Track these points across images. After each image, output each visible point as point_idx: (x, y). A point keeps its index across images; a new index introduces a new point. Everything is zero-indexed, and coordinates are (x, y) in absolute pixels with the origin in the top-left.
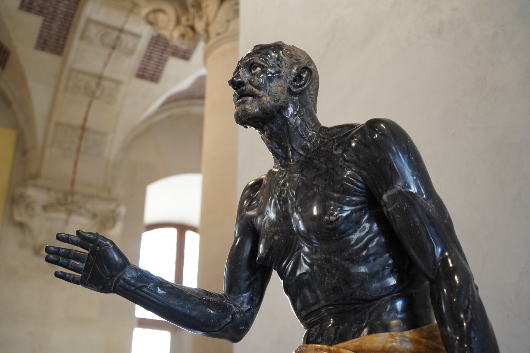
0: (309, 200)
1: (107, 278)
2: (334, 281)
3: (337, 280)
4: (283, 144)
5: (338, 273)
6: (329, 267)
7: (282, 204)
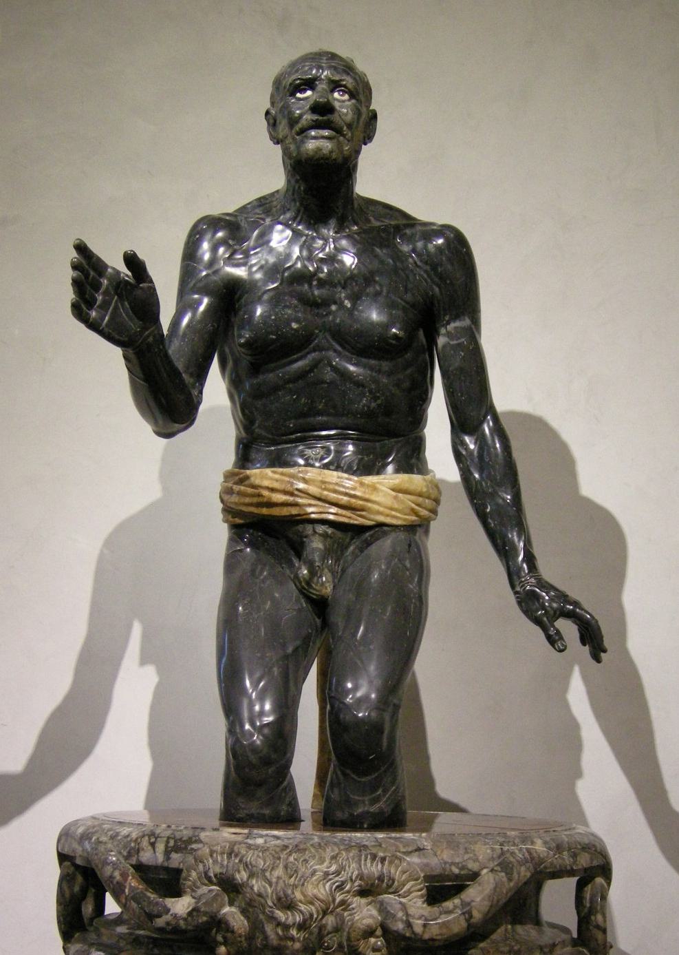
2: (373, 405)
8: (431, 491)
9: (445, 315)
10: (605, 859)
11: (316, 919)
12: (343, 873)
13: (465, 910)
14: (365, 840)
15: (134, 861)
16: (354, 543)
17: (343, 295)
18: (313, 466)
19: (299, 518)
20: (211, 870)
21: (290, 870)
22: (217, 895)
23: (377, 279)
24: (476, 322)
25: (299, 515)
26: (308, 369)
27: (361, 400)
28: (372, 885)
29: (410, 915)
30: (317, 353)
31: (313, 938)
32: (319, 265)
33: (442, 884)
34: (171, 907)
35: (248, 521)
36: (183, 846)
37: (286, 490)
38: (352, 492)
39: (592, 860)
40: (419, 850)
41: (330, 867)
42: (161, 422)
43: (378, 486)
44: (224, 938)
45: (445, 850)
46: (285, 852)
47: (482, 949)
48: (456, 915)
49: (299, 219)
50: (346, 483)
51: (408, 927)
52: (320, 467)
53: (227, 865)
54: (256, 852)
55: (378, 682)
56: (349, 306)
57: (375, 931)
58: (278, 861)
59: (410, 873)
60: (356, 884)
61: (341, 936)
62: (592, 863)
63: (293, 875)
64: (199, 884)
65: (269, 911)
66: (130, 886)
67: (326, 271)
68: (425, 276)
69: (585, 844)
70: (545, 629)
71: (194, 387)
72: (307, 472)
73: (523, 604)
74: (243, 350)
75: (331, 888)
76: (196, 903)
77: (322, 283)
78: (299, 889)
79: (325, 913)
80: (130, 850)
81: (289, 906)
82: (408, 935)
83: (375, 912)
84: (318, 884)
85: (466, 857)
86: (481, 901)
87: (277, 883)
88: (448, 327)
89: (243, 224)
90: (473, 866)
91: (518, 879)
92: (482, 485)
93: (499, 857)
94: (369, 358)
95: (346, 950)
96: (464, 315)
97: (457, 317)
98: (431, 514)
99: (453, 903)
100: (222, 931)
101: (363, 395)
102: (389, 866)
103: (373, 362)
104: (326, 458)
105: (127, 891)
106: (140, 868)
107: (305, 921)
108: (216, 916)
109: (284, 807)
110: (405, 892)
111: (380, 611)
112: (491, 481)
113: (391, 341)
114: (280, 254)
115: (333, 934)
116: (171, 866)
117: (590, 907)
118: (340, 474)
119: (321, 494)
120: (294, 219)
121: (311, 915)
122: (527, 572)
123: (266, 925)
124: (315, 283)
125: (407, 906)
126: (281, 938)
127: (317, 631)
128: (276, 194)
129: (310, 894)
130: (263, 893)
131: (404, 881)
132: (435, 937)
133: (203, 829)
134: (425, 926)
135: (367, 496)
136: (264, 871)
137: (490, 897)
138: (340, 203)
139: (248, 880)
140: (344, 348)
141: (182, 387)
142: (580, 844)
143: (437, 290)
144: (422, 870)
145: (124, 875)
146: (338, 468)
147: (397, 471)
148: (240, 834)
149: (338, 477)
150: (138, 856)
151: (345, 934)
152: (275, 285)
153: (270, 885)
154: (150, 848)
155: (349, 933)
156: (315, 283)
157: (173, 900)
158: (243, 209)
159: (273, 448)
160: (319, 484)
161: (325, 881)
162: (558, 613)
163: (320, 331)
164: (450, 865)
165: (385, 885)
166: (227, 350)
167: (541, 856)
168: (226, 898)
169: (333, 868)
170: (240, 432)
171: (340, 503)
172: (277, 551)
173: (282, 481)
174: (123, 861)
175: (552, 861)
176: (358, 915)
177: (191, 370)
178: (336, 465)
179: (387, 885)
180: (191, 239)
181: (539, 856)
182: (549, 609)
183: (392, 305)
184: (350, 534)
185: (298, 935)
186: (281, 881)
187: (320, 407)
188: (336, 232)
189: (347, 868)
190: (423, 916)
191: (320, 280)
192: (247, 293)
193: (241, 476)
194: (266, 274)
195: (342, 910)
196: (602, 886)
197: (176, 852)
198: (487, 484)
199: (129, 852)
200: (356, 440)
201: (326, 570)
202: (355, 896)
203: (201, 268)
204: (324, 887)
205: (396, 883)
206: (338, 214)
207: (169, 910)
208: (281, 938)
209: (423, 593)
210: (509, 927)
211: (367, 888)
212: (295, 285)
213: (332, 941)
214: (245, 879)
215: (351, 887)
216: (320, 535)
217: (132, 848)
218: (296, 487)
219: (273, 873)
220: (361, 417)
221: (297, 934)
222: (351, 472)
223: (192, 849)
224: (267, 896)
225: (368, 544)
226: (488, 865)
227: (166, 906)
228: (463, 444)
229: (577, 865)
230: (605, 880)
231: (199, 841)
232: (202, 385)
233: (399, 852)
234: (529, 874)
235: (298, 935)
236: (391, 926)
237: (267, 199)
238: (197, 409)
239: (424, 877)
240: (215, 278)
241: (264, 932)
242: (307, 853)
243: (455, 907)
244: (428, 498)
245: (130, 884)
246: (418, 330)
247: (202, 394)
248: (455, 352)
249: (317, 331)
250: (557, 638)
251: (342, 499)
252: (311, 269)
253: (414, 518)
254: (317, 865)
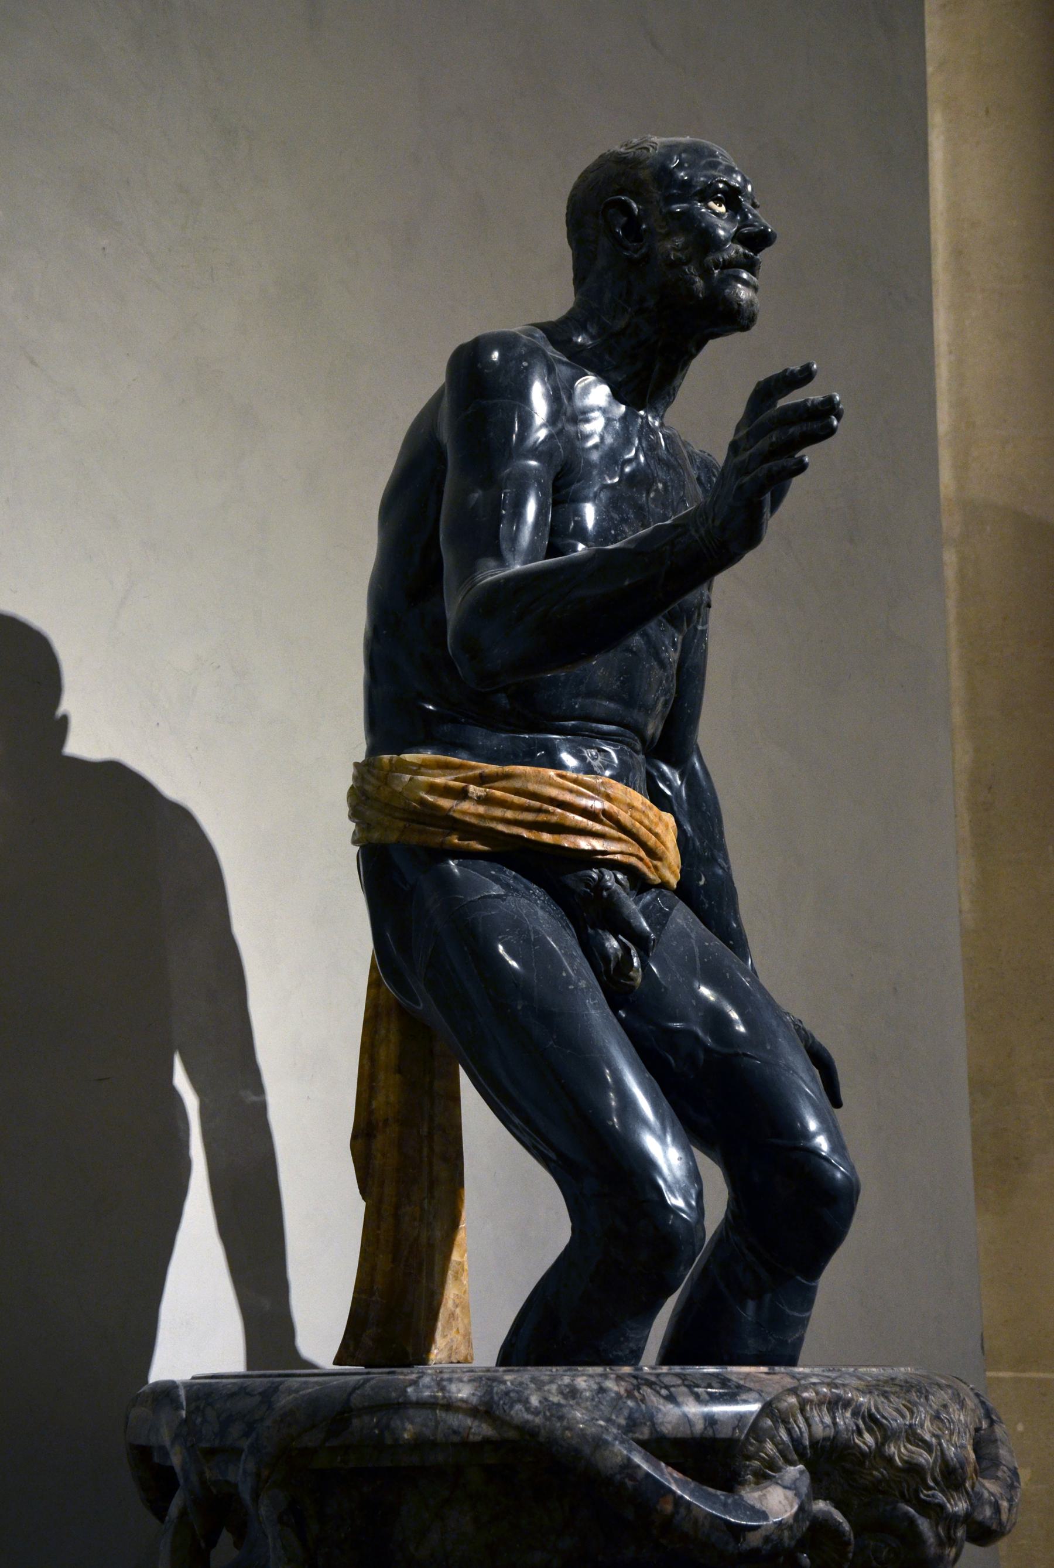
64: (781, 1462)
116: (719, 1436)
198: (702, 843)
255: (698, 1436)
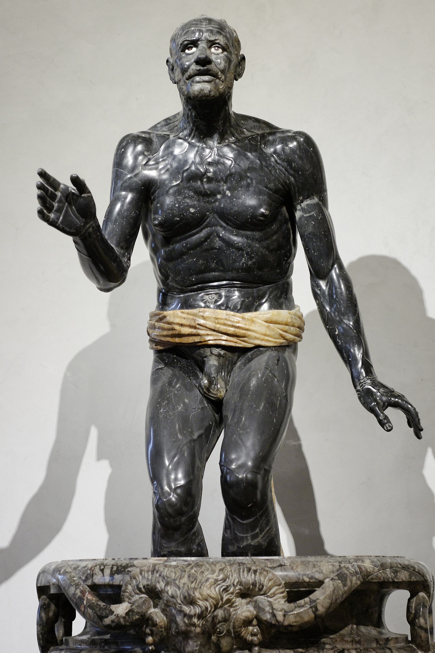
0: (242, 189)
1: (81, 223)
2: (250, 263)
3: (253, 262)
4: (215, 124)
5: (256, 257)
6: (249, 250)
7: (205, 182)
8: (294, 321)
9: (299, 197)
10: (423, 577)
11: (210, 611)
12: (228, 580)
13: (312, 605)
14: (245, 560)
15: (89, 582)
16: (241, 360)
17: (225, 187)
18: (209, 307)
19: (200, 344)
20: (141, 584)
21: (193, 578)
22: (145, 600)
23: (249, 175)
24: (323, 200)
25: (200, 342)
26: (203, 239)
27: (241, 260)
28: (249, 589)
29: (275, 609)
30: (209, 228)
31: (209, 624)
32: (207, 167)
33: (299, 589)
34: (115, 611)
35: (166, 347)
36: (122, 570)
37: (191, 325)
38: (237, 325)
39: (410, 576)
40: (281, 566)
41: (219, 576)
42: (101, 282)
43: (255, 319)
44: (151, 630)
45: (299, 566)
46: (189, 567)
47: (331, 638)
48: (306, 608)
49: (193, 135)
50: (232, 318)
51: (273, 617)
52: (214, 308)
53: (151, 579)
54: (170, 569)
55: (252, 454)
56: (229, 195)
57: (252, 620)
58: (184, 573)
59: (274, 581)
60: (238, 588)
61: (229, 625)
62: (411, 579)
63: (193, 581)
65: (178, 607)
66: (87, 599)
67: (212, 170)
68: (283, 169)
69: (405, 565)
70: (377, 416)
71: (124, 255)
72: (205, 312)
73: (362, 399)
74: (157, 228)
75: (220, 590)
76: (131, 606)
77: (210, 180)
78: (198, 590)
79: (216, 607)
80: (87, 575)
81: (191, 602)
82: (273, 622)
83: (252, 609)
84: (210, 587)
85: (314, 570)
86: (324, 599)
87: (183, 587)
88: (302, 204)
89: (155, 140)
90: (318, 576)
91: (351, 585)
92: (331, 315)
93: (338, 571)
94: (245, 230)
95: (233, 635)
96: (313, 195)
97: (308, 197)
98: (295, 337)
99: (304, 601)
100: (149, 626)
101: (243, 256)
102: (259, 576)
103: (248, 233)
104: (219, 301)
105: (85, 602)
106: (94, 588)
107: (202, 612)
108: (145, 615)
109: (195, 547)
110: (271, 594)
111: (254, 406)
112: (338, 313)
113: (260, 218)
114: (180, 160)
115: (223, 623)
116: (114, 584)
117: (415, 613)
118: (228, 312)
119: (214, 327)
120: (190, 135)
121: (207, 608)
122: (364, 375)
123: (177, 617)
124: (205, 180)
125: (273, 603)
126: (187, 625)
127: (216, 422)
128: (177, 116)
129: (205, 593)
130: (175, 595)
131: (270, 586)
132: (292, 624)
133: (136, 559)
134: (284, 616)
135: (247, 327)
136: (175, 580)
137: (330, 597)
138: (220, 123)
139: (165, 587)
140: (227, 224)
141: (115, 258)
142: (401, 565)
143: (292, 179)
144: (283, 579)
145: (83, 592)
146: (227, 308)
147: (271, 308)
148: (161, 560)
149: (227, 315)
150: (92, 579)
151: (232, 624)
152: (178, 182)
153: (179, 588)
154: (100, 573)
155: (234, 623)
156: (205, 180)
157: (116, 605)
158: (155, 127)
159: (182, 296)
160: (214, 320)
161: (215, 585)
162: (386, 403)
163: (210, 213)
164: (302, 576)
165: (257, 589)
166: (147, 226)
167: (369, 570)
168: (152, 603)
169: (221, 576)
170: (159, 284)
171: (228, 332)
172: (187, 367)
173: (188, 319)
174: (83, 583)
175: (378, 574)
176: (240, 610)
177: (122, 244)
178: (225, 306)
179: (259, 588)
180: (119, 152)
181: (366, 570)
182: (380, 401)
183: (259, 193)
184: (237, 354)
185: (199, 623)
186: (186, 586)
187: (213, 266)
188: (219, 143)
189: (231, 577)
190: (284, 609)
191: (208, 178)
192: (158, 189)
193: (161, 316)
194: (171, 174)
195: (229, 606)
196: (424, 598)
197: (118, 574)
199: (86, 577)
200: (239, 288)
201: (220, 380)
202: (237, 597)
203: (126, 173)
204: (215, 590)
205: (265, 587)
206: (219, 130)
207: (113, 612)
208: (187, 625)
209: (289, 394)
210: (355, 626)
211: (245, 591)
212: (191, 182)
213: (222, 627)
214: (163, 587)
215: (234, 590)
216: (215, 355)
217: (88, 574)
218: (197, 322)
219: (181, 581)
220: (242, 272)
221: (198, 622)
222: (236, 311)
223: (128, 571)
224: (177, 597)
225: (250, 360)
226: (329, 576)
227: (111, 610)
228: (319, 286)
229: (398, 578)
230: (426, 594)
231: (133, 566)
232: (130, 254)
233: (267, 567)
234: (359, 582)
235: (199, 623)
236: (262, 617)
237: (171, 120)
238: (126, 271)
239: (285, 584)
240: (136, 179)
241: (176, 623)
242: (203, 567)
243: (306, 603)
244: (293, 326)
245: (87, 597)
246: (282, 208)
247: (130, 260)
248: (307, 222)
249: (208, 213)
250: (386, 421)
251: (230, 330)
252: (201, 170)
253: (282, 341)
254: (210, 575)
255: (107, 584)
